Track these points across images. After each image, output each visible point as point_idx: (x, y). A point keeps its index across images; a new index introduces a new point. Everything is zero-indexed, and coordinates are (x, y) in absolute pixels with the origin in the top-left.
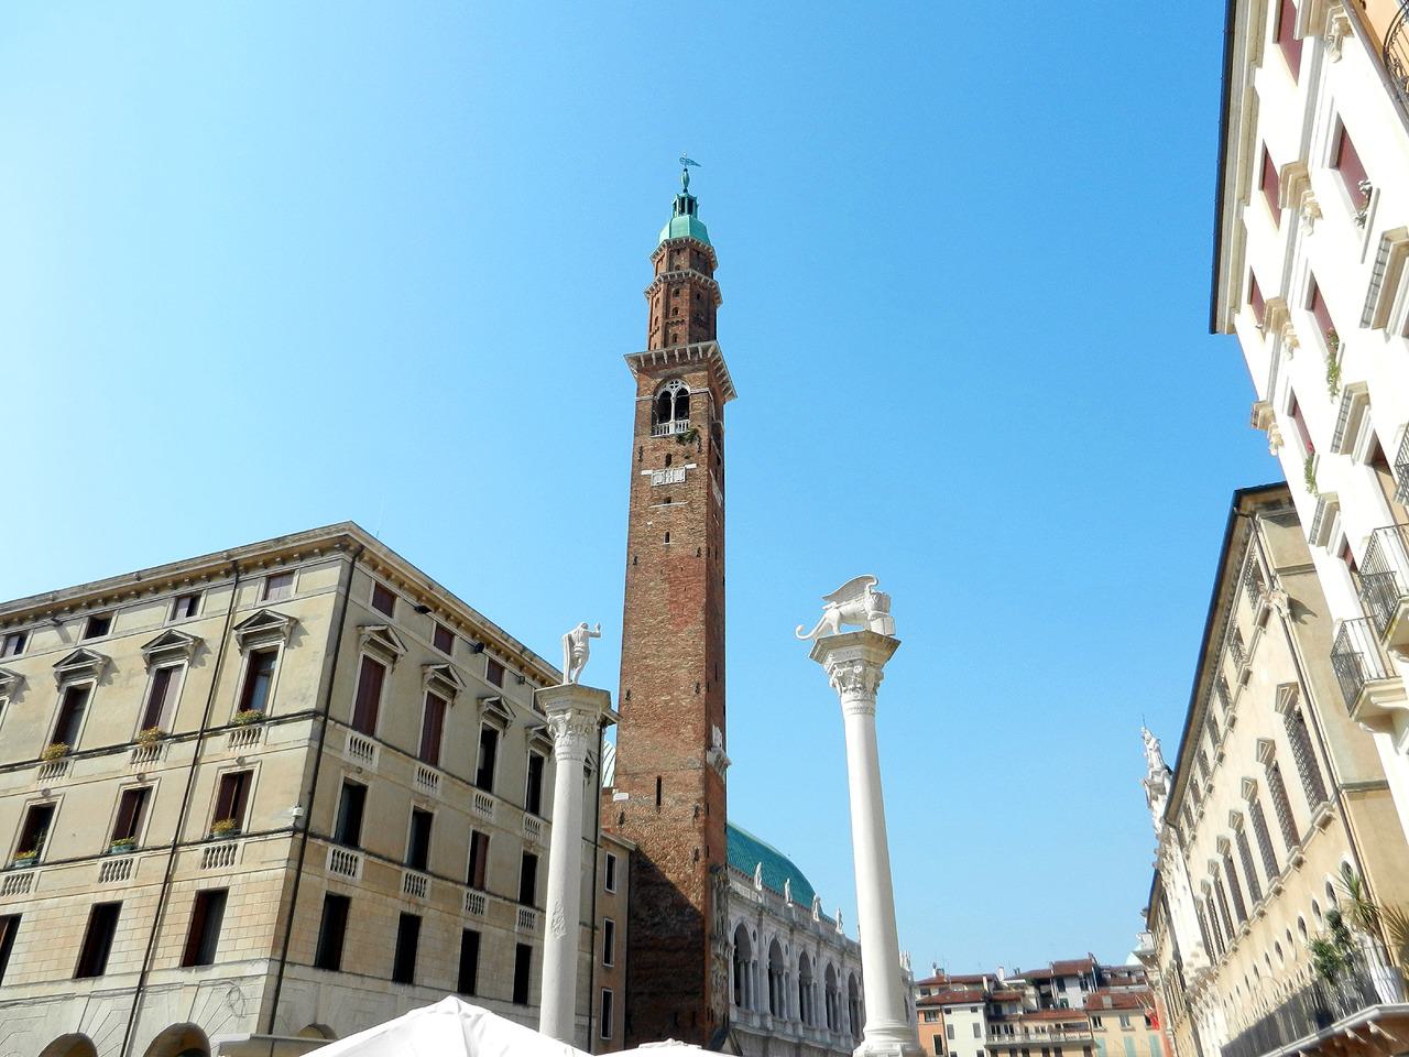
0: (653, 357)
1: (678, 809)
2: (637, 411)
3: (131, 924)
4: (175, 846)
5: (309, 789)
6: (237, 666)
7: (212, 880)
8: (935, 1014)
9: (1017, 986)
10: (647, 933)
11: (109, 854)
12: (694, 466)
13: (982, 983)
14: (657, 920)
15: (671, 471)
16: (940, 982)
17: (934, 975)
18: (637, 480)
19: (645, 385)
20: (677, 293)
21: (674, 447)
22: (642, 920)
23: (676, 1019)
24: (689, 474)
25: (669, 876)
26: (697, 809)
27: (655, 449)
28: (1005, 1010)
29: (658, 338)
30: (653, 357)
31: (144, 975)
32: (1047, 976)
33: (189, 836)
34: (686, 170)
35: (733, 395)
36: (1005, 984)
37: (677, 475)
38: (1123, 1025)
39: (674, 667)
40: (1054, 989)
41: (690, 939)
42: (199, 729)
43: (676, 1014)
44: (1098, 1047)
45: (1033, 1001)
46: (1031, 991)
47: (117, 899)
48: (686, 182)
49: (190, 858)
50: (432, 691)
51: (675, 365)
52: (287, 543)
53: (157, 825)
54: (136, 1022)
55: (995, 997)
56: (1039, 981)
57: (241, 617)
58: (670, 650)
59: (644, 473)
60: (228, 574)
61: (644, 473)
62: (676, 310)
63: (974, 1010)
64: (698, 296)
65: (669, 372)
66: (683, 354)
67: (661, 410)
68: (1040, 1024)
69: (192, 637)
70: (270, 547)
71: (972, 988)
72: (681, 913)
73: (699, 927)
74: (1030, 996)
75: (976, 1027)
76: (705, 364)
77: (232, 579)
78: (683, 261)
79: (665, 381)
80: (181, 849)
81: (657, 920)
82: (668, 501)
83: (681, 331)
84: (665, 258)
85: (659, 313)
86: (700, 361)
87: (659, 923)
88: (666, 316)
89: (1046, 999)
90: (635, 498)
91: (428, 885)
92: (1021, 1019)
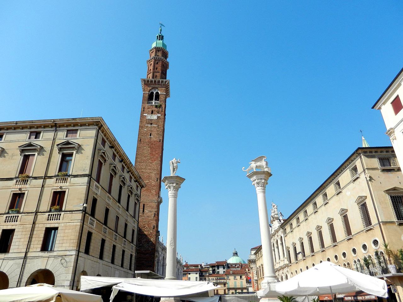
0: (150, 81)
1: (149, 214)
2: (143, 96)
3: (19, 237)
4: (37, 213)
5: (86, 198)
6: (57, 158)
7: (52, 224)
8: (186, 274)
9: (207, 267)
11: (8, 213)
12: (160, 115)
13: (198, 266)
14: (141, 245)
16: (187, 266)
17: (185, 264)
18: (142, 116)
19: (146, 89)
20: (157, 63)
21: (154, 109)
24: (158, 117)
25: (145, 233)
26: (155, 214)
27: (148, 108)
28: (204, 274)
29: (151, 75)
30: (150, 81)
31: (26, 253)
32: (214, 265)
33: (41, 209)
34: (161, 27)
35: (169, 96)
36: (204, 267)
37: (154, 117)
38: (234, 278)
39: (151, 173)
40: (216, 268)
41: (151, 251)
42: (44, 176)
44: (228, 284)
45: (211, 272)
46: (211, 269)
47: (13, 228)
48: (161, 31)
49: (42, 218)
50: (111, 173)
51: (156, 84)
52: (77, 120)
53: (28, 204)
54: (23, 268)
55: (202, 270)
56: (213, 266)
57: (58, 142)
58: (149, 168)
59: (144, 115)
60: (52, 127)
61: (144, 115)
62: (157, 68)
63: (197, 274)
64: (163, 66)
65: (154, 86)
66: (159, 82)
67: (150, 97)
68: (213, 278)
69: (39, 146)
70: (70, 121)
71: (195, 268)
72: (148, 244)
73: (153, 247)
74: (211, 270)
75: (196, 278)
76: (165, 86)
77: (54, 129)
78: (160, 54)
79: (152, 89)
80: (38, 214)
82: (151, 124)
83: (158, 75)
84: (154, 52)
85: (151, 68)
86: (164, 85)
87: (142, 246)
88: (154, 69)
89: (214, 271)
90: (141, 122)
91: (107, 231)
92: (208, 276)
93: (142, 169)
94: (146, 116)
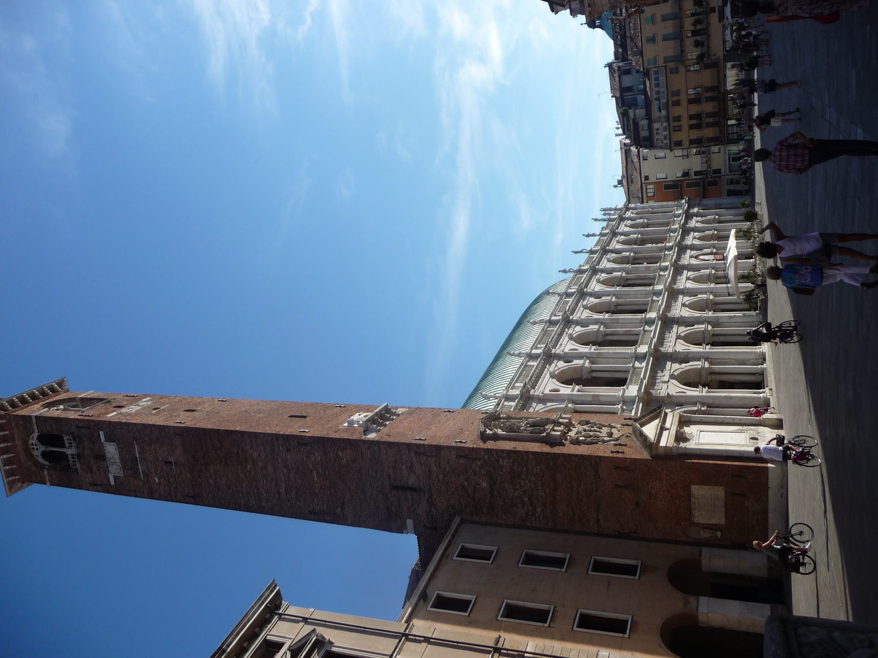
10: (539, 510)
14: (526, 499)
15: (108, 455)
22: (527, 514)
23: (621, 486)
24: (109, 439)
37: (111, 450)
43: (617, 486)
58: (270, 469)
59: (112, 483)
61: (112, 483)
81: (526, 499)
93: (279, 493)
94: (115, 478)
